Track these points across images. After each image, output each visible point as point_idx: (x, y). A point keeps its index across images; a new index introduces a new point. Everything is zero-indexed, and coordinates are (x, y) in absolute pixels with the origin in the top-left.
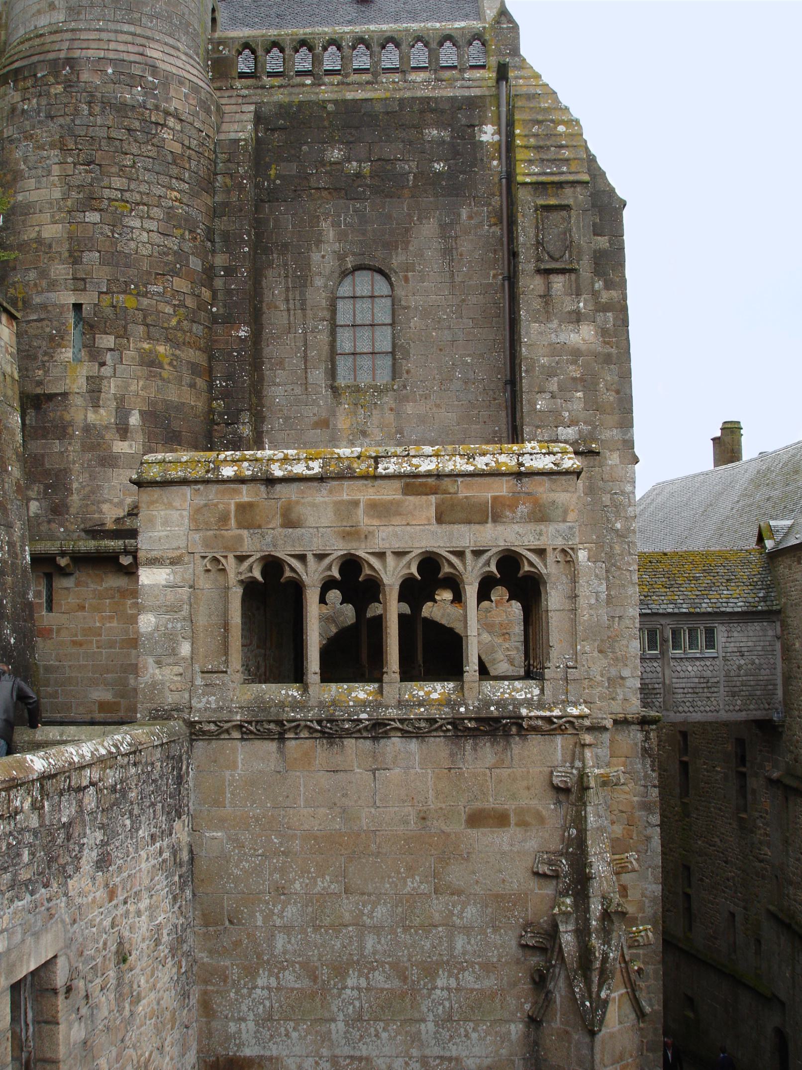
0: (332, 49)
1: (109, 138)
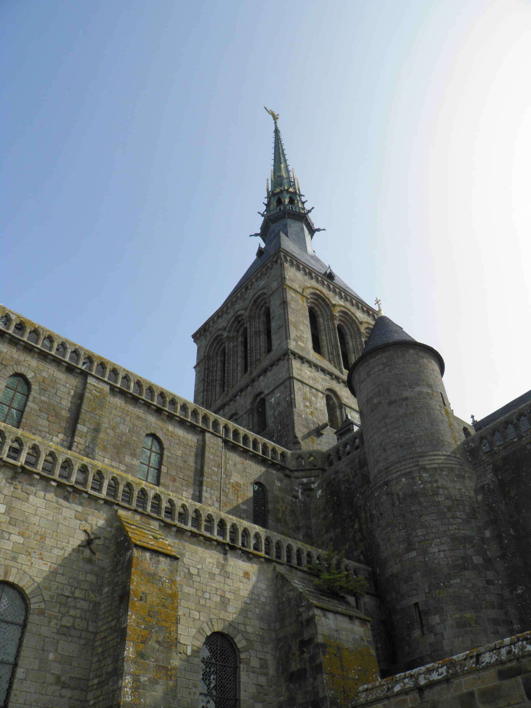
0: (523, 418)
1: (411, 511)
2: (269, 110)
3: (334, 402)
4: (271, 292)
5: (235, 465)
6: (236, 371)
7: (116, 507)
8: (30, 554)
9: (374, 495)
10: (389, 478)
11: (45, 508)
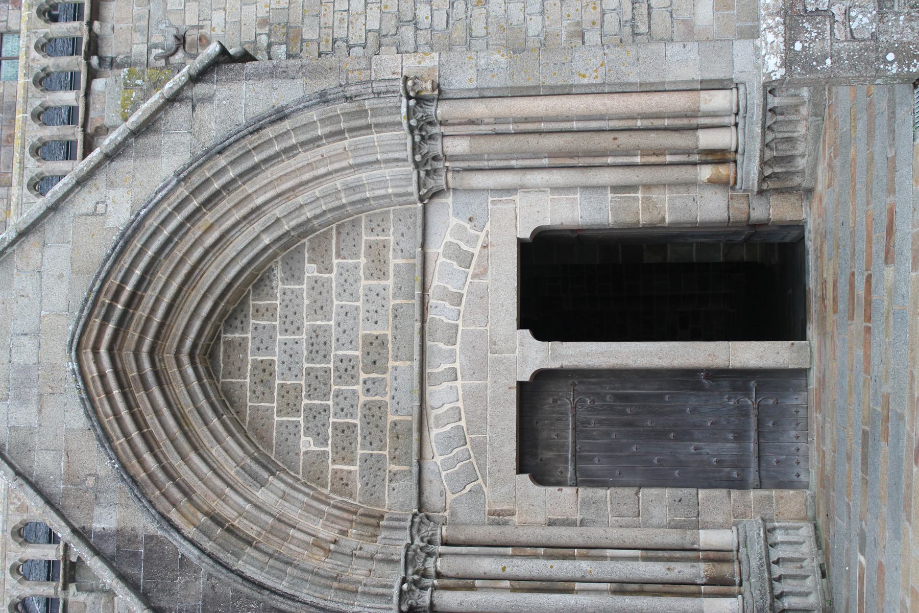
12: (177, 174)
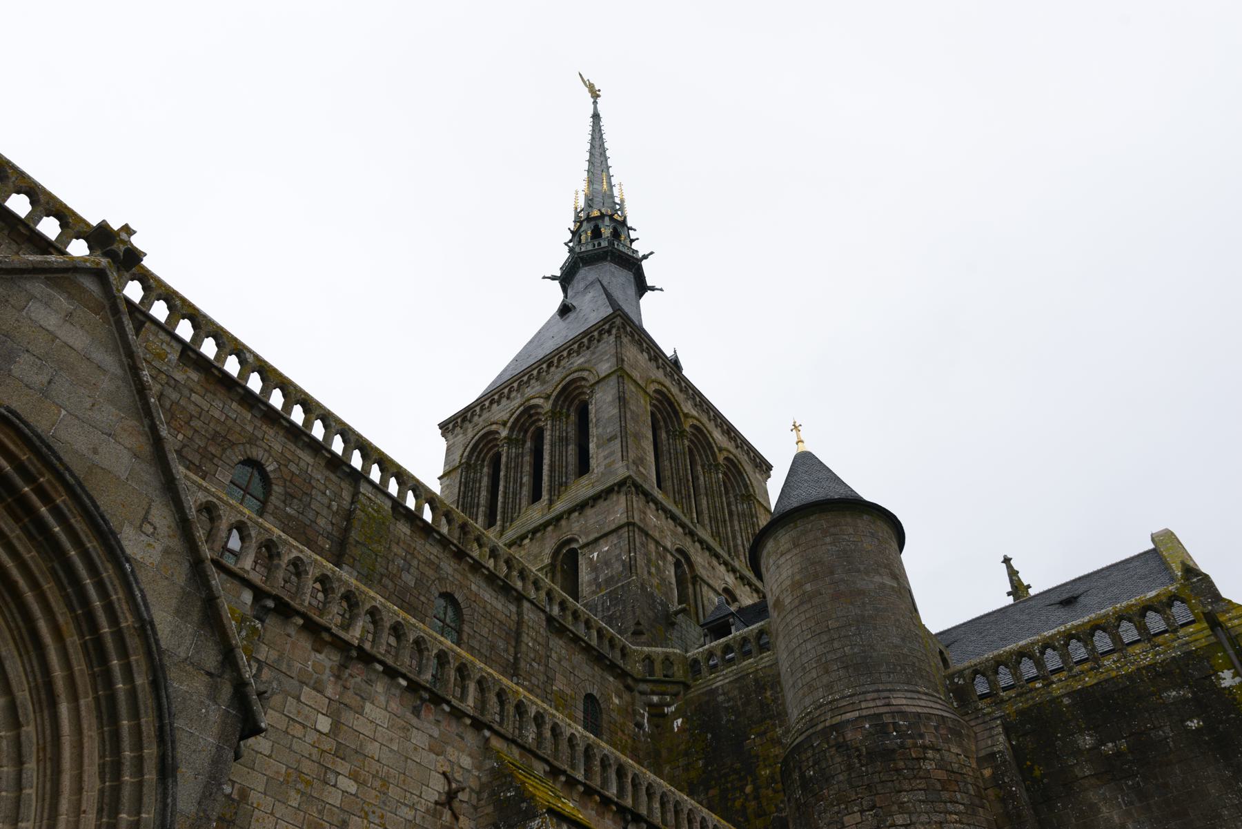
0: (1049, 651)
2: (586, 80)
3: (684, 572)
4: (597, 379)
5: (559, 662)
6: (518, 496)
7: (487, 733)
8: (367, 814)
9: (812, 746)
10: (838, 719)
11: (387, 728)
12: (152, 623)
